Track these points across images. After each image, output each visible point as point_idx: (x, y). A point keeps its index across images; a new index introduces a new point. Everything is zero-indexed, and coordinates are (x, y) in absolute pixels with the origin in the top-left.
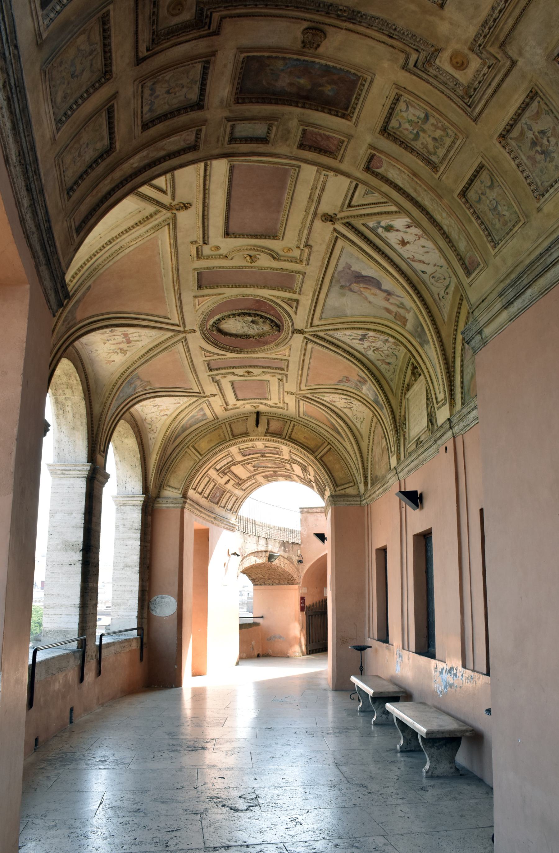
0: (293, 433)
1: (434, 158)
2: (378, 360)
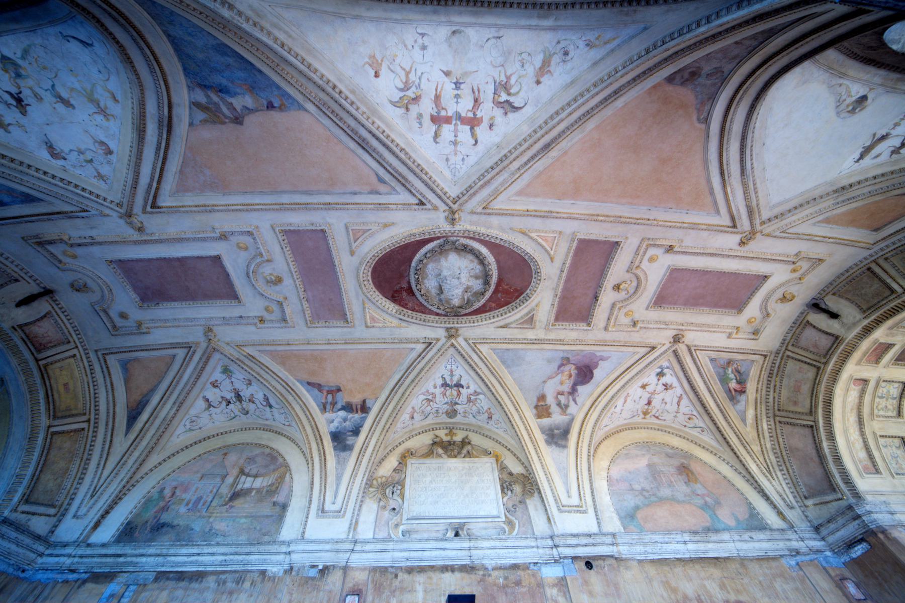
0: (58, 365)
1: (876, 411)
2: (413, 408)
